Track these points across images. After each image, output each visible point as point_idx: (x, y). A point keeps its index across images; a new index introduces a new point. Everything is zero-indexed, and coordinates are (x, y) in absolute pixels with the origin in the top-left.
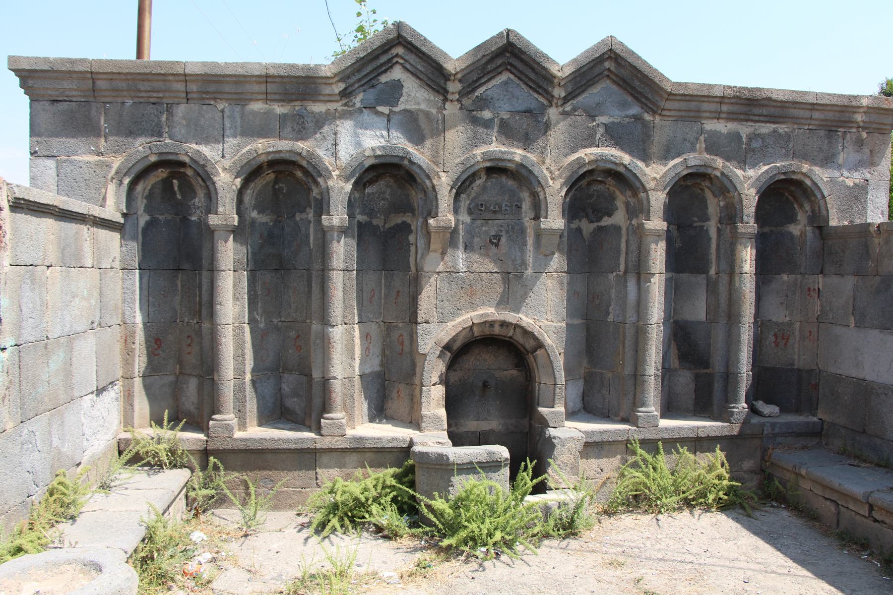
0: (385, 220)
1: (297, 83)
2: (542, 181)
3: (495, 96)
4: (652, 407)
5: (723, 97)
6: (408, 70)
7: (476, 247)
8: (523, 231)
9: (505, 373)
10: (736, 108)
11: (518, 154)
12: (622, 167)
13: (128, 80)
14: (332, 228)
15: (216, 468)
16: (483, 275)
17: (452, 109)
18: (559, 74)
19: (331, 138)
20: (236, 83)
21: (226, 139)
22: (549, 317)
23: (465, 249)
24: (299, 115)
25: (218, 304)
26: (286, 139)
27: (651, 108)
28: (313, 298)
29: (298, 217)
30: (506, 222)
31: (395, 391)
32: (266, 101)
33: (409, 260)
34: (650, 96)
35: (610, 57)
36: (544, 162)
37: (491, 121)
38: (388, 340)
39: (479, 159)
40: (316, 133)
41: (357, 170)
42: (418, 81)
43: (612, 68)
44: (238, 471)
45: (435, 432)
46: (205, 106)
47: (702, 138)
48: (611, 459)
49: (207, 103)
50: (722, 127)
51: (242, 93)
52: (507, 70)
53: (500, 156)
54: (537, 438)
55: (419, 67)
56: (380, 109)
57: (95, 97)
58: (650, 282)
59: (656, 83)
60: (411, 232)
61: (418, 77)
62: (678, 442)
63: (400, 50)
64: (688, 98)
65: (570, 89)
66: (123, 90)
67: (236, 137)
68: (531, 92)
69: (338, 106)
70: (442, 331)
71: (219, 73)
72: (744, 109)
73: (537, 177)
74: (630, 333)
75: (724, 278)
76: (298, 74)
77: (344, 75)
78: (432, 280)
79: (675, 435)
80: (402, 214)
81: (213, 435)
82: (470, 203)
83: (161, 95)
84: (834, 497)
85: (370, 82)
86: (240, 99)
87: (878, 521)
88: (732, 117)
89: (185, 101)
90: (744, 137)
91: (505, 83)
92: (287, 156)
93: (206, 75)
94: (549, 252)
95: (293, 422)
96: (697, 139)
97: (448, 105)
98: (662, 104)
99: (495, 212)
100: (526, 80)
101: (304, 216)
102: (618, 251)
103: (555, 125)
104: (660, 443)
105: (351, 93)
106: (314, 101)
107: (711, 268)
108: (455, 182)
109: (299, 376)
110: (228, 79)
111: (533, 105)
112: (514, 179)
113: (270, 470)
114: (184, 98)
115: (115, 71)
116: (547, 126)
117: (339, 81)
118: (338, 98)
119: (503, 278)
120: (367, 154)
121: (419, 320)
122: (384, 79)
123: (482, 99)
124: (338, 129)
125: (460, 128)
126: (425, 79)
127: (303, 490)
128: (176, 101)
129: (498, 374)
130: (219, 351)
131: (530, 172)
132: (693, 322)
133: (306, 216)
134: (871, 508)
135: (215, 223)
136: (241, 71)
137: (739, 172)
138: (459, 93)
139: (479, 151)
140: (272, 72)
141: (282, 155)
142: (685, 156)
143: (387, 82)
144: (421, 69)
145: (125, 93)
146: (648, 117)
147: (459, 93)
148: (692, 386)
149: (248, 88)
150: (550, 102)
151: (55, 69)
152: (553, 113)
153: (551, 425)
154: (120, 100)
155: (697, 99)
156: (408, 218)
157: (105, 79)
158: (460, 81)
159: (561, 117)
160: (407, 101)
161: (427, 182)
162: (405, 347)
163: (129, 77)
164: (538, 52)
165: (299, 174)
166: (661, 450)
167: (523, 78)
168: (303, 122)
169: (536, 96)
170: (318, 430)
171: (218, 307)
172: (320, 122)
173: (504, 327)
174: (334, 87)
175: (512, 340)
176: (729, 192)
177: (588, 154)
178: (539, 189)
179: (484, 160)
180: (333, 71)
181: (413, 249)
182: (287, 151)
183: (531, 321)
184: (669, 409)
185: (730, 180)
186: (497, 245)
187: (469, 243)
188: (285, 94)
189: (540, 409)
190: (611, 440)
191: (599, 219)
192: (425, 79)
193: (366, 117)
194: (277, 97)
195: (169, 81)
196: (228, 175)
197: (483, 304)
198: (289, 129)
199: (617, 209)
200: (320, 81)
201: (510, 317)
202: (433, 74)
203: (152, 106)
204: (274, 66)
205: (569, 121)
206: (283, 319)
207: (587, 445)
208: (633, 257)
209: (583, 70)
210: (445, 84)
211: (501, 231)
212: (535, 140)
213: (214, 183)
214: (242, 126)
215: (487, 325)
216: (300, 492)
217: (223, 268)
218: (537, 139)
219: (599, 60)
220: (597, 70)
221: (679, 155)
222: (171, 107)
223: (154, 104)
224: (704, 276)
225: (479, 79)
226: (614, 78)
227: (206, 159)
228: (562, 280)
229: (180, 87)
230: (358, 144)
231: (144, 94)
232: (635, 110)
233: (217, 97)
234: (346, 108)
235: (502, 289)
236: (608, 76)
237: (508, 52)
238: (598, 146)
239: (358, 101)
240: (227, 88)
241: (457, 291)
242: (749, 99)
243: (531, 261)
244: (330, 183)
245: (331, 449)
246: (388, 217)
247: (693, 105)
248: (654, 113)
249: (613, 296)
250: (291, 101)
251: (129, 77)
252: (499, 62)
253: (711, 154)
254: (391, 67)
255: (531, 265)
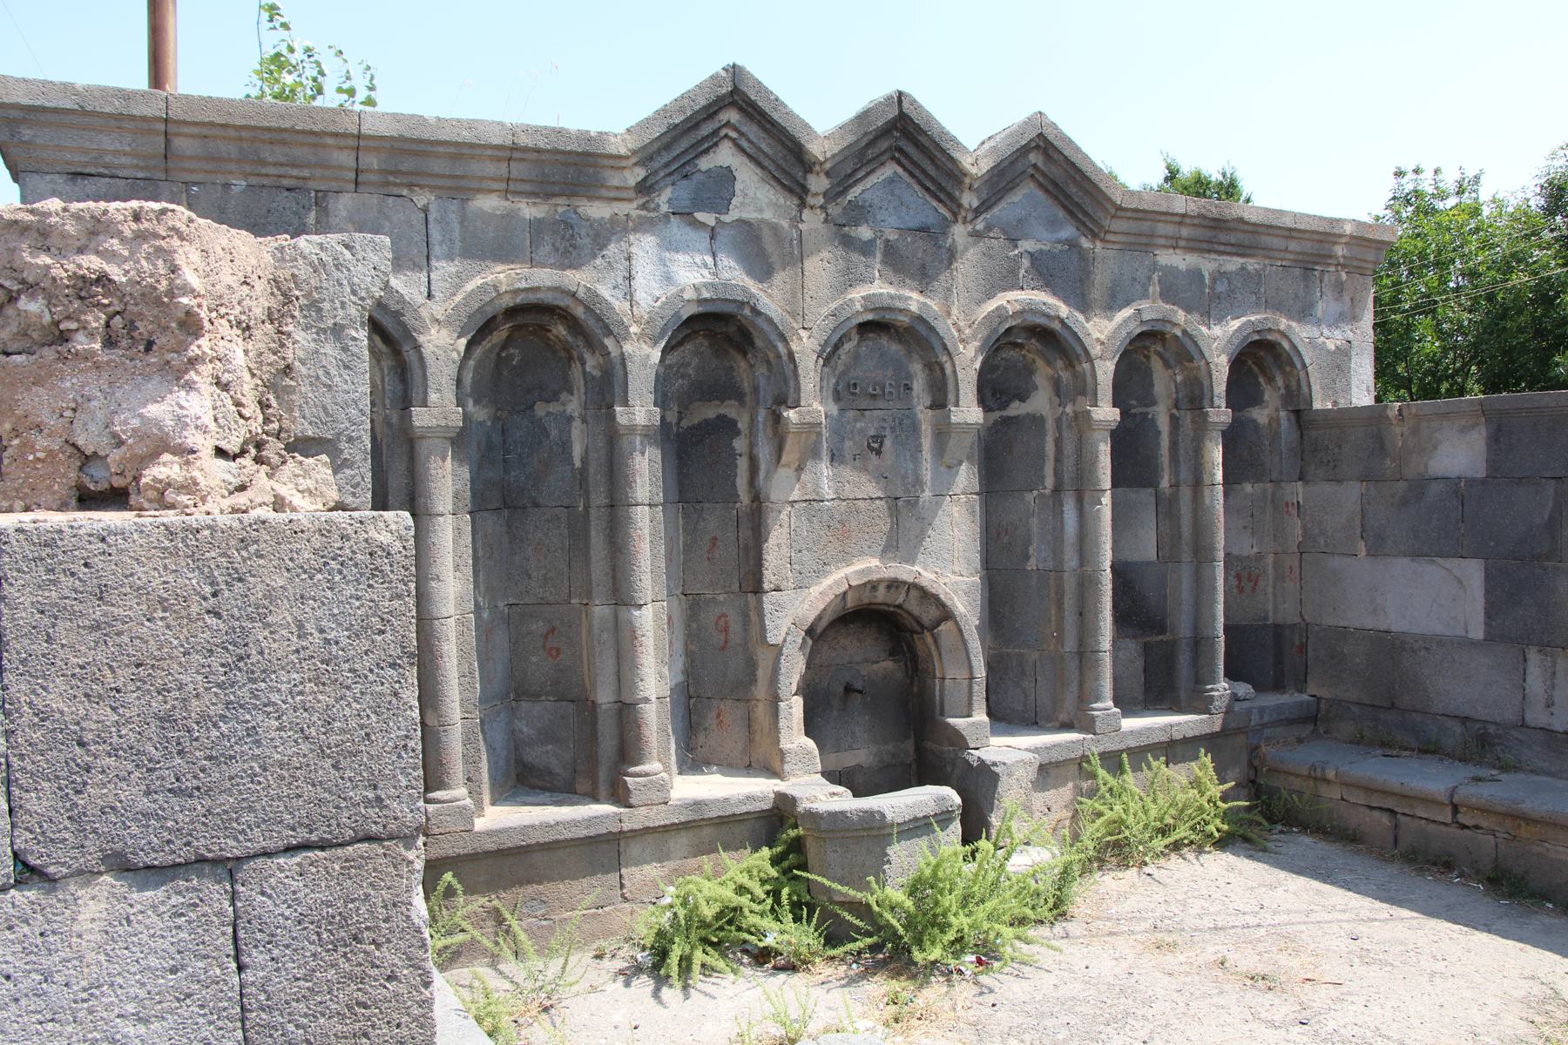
0: (680, 413)
1: (563, 164)
2: (949, 345)
3: (876, 201)
4: (1105, 705)
5: (1184, 216)
6: (743, 151)
7: (848, 457)
8: (915, 429)
9: (875, 666)
10: (1199, 233)
11: (914, 300)
12: (1057, 322)
13: (240, 139)
14: (632, 429)
15: (450, 892)
16: (860, 503)
17: (812, 221)
18: (974, 170)
19: (621, 267)
20: (454, 157)
21: (434, 263)
22: (957, 568)
23: (832, 461)
24: (566, 223)
25: (433, 579)
26: (544, 266)
27: (1091, 230)
28: (594, 559)
29: (540, 410)
30: (890, 413)
31: (714, 714)
32: (506, 193)
33: (734, 484)
34: (1090, 211)
35: (1038, 147)
36: (949, 314)
37: (872, 242)
38: (694, 625)
39: (858, 307)
40: (594, 256)
41: (670, 325)
42: (758, 171)
43: (1040, 164)
44: (482, 893)
45: (806, 778)
46: (391, 199)
47: (1155, 277)
48: (1061, 790)
49: (395, 193)
50: (1180, 261)
51: (463, 177)
52: (893, 158)
53: (887, 302)
54: (949, 769)
55: (763, 146)
56: (700, 216)
57: (166, 171)
58: (1101, 504)
59: (1101, 191)
60: (738, 433)
61: (759, 164)
62: (1149, 751)
63: (732, 115)
64: (1140, 215)
65: (984, 196)
66: (230, 160)
67: (453, 260)
68: (927, 197)
69: (630, 208)
70: (802, 602)
71: (426, 136)
72: (1208, 234)
73: (941, 339)
74: (1070, 585)
75: (1186, 493)
76: (569, 148)
77: (645, 156)
78: (783, 516)
79: (1144, 741)
80: (717, 402)
81: (437, 831)
82: (837, 382)
83: (306, 173)
84: (1389, 803)
85: (682, 169)
86: (457, 189)
87: (1468, 827)
88: (1194, 246)
89: (352, 186)
90: (1207, 276)
91: (891, 181)
92: (548, 298)
93: (402, 139)
94: (955, 462)
95: (549, 790)
96: (1150, 279)
97: (806, 214)
98: (1106, 223)
99: (874, 396)
100: (922, 177)
101: (553, 408)
102: (1042, 457)
103: (963, 253)
104: (1124, 755)
105: (651, 186)
106: (591, 198)
107: (1162, 477)
108: (823, 347)
109: (557, 704)
110: (441, 149)
111: (931, 220)
112: (900, 341)
113: (540, 883)
114: (349, 181)
115: (218, 120)
116: (952, 255)
117: (635, 164)
118: (632, 194)
119: (889, 508)
120: (686, 296)
121: (766, 586)
122: (705, 164)
123: (857, 206)
124: (633, 249)
125: (825, 254)
126: (772, 168)
127: (600, 911)
128: (334, 185)
129: (865, 670)
130: (438, 668)
131: (932, 329)
132: (1136, 563)
133: (561, 408)
134: (1455, 809)
135: (425, 424)
136: (466, 136)
137: (1204, 329)
138: (825, 194)
139: (858, 294)
140: (524, 140)
141: (541, 296)
142: (1135, 305)
143: (709, 170)
144: (766, 149)
145: (233, 166)
146: (1085, 243)
147: (825, 194)
148: (1140, 663)
149: (476, 168)
150: (955, 215)
151: (89, 108)
152: (959, 232)
153: (972, 746)
154: (220, 179)
155: (1152, 216)
156: (730, 409)
157: (192, 136)
158: (828, 174)
159: (970, 239)
160: (742, 204)
161: (781, 347)
162: (731, 635)
163: (245, 134)
164: (943, 133)
165: (560, 330)
166: (1127, 767)
167: (917, 173)
168: (572, 236)
169: (935, 203)
170: (619, 795)
171: (433, 584)
172: (602, 235)
173: (893, 590)
174: (627, 173)
175: (899, 611)
176: (1191, 359)
177: (1012, 300)
178: (944, 358)
179: (867, 310)
180: (630, 146)
181: (743, 464)
182: (549, 289)
183: (932, 576)
184: (1128, 704)
185: (1195, 343)
186: (878, 452)
187: (838, 450)
188: (542, 182)
189: (951, 720)
190: (1061, 759)
191: (1004, 406)
192: (772, 168)
193: (675, 230)
194: (527, 187)
195: (324, 146)
196: (444, 332)
197: (862, 553)
198: (548, 248)
199: (1036, 388)
200: (606, 162)
201: (904, 572)
202: (786, 161)
203: (286, 193)
204: (526, 130)
205: (982, 246)
206: (512, 601)
207: (1043, 769)
208: (1069, 464)
209: (1003, 165)
210: (805, 179)
211: (884, 428)
212: (934, 278)
213: (418, 347)
214: (463, 240)
215: (869, 587)
216: (594, 915)
217: (440, 509)
218: (938, 275)
219: (1024, 151)
220: (1020, 167)
221: (1127, 304)
222: (324, 197)
223: (288, 190)
224: (1151, 490)
225: (855, 171)
226: (1041, 179)
227: (401, 300)
228: (973, 507)
229: (347, 159)
230: (668, 278)
231: (271, 170)
232: (1068, 232)
233: (415, 182)
234: (644, 213)
235: (889, 526)
236: (1032, 176)
237: (897, 129)
238: (1022, 289)
239: (664, 199)
240: (438, 166)
241: (822, 533)
242: (1215, 220)
243: (929, 477)
244: (628, 348)
245: (648, 828)
246: (687, 408)
247: (1145, 226)
248: (1095, 236)
249: (1035, 530)
250: (549, 196)
251: (245, 134)
252: (884, 144)
253: (1167, 303)
254: (716, 144)
255: (929, 484)
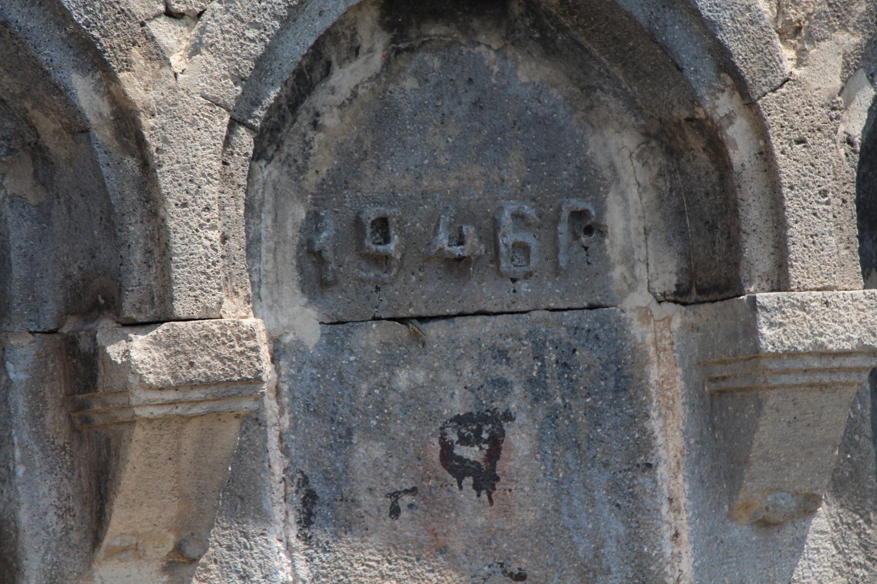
23: (307, 520)
30: (522, 325)
82: (314, 220)
211: (502, 384)
243: (686, 565)
